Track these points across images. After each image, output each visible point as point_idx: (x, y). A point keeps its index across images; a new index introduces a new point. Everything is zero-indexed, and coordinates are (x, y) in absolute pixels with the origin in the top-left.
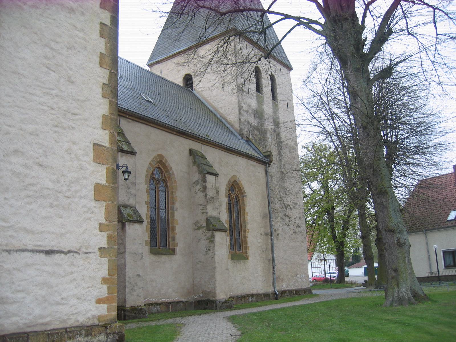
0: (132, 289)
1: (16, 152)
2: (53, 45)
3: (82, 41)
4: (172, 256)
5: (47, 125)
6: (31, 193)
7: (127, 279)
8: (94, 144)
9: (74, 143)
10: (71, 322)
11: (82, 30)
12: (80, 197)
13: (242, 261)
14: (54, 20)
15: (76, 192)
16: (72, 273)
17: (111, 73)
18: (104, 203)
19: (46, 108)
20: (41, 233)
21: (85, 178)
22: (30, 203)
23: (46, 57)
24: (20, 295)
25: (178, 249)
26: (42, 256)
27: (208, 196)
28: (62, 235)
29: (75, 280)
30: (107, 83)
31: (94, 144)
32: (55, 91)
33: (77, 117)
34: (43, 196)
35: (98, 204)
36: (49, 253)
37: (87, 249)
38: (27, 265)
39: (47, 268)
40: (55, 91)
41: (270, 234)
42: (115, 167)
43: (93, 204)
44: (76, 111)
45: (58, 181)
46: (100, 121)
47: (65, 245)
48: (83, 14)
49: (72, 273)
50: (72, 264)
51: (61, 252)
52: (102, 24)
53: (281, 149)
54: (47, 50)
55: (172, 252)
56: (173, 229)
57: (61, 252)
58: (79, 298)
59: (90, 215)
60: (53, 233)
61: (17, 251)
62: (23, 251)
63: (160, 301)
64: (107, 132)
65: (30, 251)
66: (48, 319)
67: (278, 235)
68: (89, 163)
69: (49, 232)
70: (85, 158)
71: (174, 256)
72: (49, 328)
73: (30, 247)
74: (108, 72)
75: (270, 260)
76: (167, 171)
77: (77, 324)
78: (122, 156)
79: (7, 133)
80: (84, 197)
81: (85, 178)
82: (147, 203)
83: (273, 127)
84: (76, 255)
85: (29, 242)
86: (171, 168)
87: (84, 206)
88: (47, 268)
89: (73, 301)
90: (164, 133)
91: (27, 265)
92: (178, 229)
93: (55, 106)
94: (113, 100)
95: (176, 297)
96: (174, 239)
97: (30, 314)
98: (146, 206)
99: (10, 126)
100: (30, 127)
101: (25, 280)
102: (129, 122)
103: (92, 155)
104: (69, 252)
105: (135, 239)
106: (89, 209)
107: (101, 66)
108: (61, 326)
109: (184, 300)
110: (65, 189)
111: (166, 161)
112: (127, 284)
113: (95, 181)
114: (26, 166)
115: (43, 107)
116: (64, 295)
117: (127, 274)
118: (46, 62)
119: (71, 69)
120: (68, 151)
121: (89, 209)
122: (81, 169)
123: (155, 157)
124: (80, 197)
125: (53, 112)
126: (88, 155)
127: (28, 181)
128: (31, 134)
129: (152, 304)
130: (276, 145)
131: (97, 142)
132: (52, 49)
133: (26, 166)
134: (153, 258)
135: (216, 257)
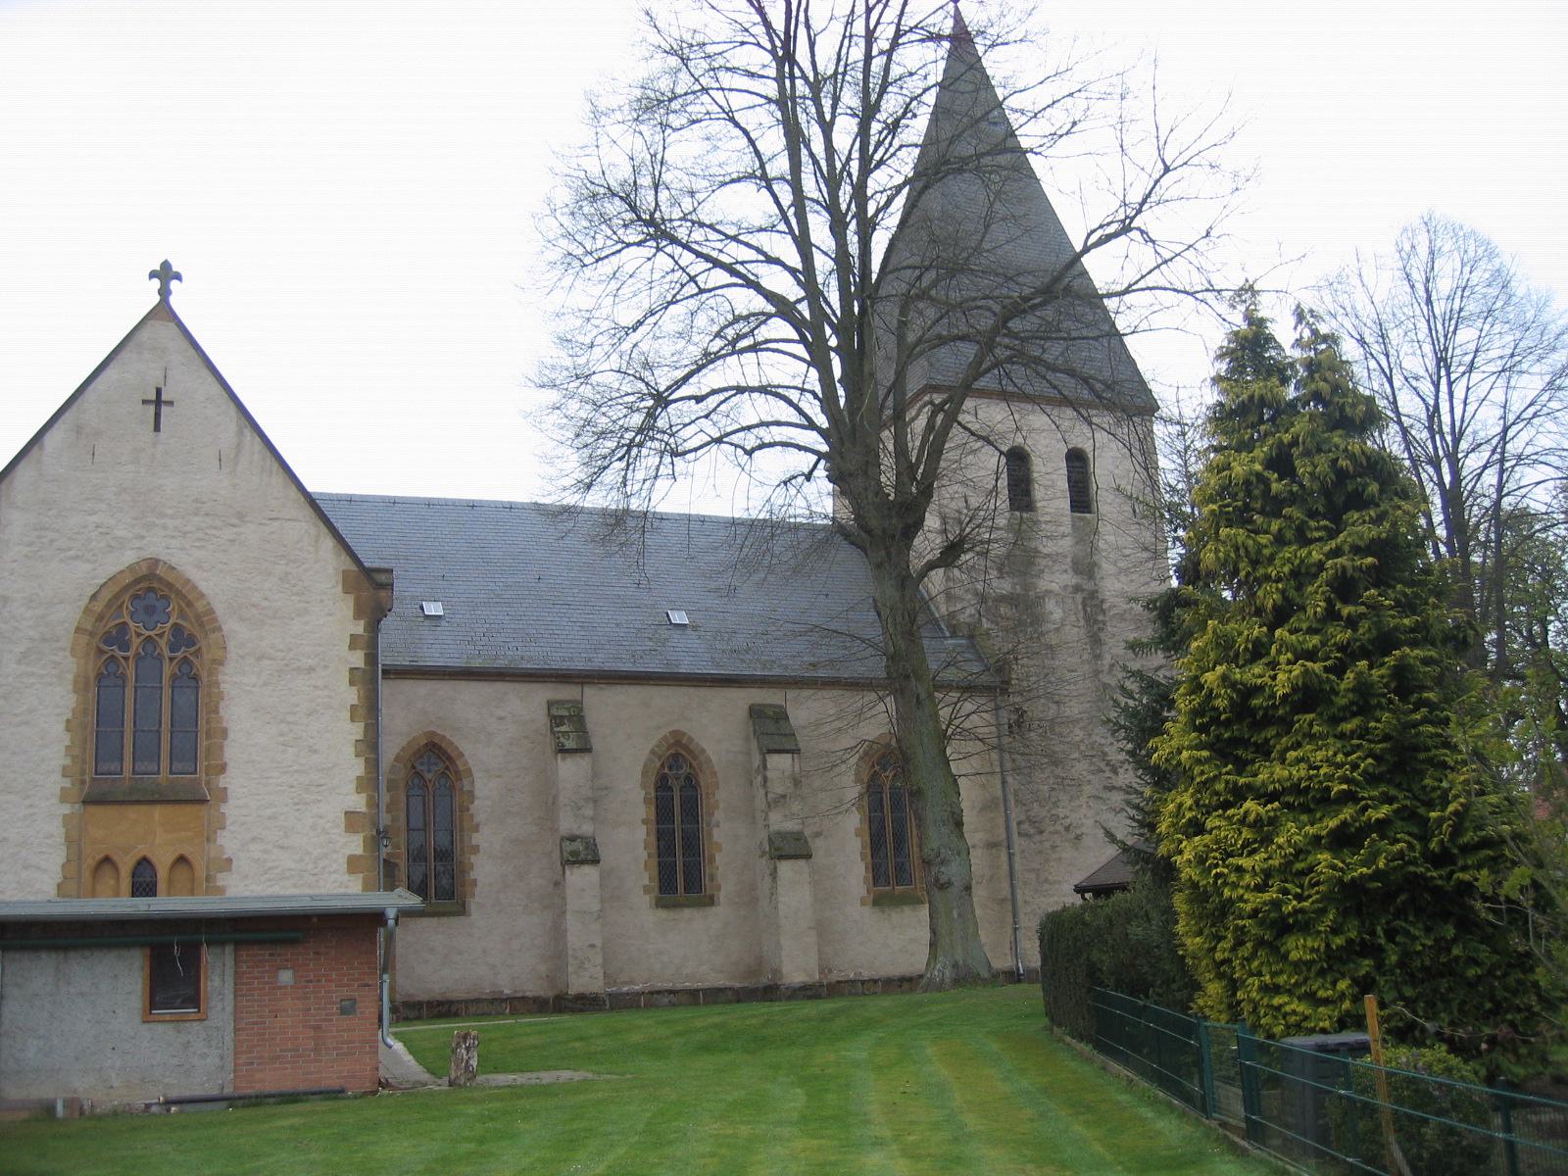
0: (580, 967)
1: (254, 839)
3: (326, 700)
4: (708, 908)
5: (286, 805)
7: (570, 952)
9: (321, 817)
11: (326, 687)
12: (330, 873)
13: (905, 908)
15: (324, 868)
18: (361, 875)
22: (271, 886)
25: (722, 896)
27: (769, 796)
30: (360, 737)
34: (287, 878)
35: (353, 877)
41: (1005, 844)
42: (374, 833)
43: (347, 877)
44: (322, 781)
46: (353, 786)
48: (326, 667)
53: (1101, 630)
55: (711, 901)
56: (712, 859)
63: (679, 986)
64: (364, 795)
67: (1078, 837)
68: (340, 835)
70: (335, 831)
71: (713, 909)
74: (362, 725)
75: (1003, 901)
76: (695, 758)
78: (564, 759)
80: (334, 872)
81: (335, 851)
82: (645, 822)
83: (1070, 579)
86: (703, 751)
87: (335, 882)
90: (684, 690)
92: (720, 859)
93: (295, 783)
94: (372, 756)
95: (719, 980)
96: (712, 878)
98: (645, 827)
100: (269, 812)
102: (602, 689)
105: (583, 890)
106: (341, 883)
109: (738, 985)
110: (310, 867)
111: (691, 740)
112: (570, 959)
113: (348, 852)
114: (265, 851)
117: (569, 945)
118: (281, 739)
119: (312, 738)
120: (313, 827)
123: (665, 738)
124: (330, 873)
129: (658, 992)
130: (1082, 623)
132: (289, 723)
133: (265, 851)
134: (662, 914)
135: (780, 906)
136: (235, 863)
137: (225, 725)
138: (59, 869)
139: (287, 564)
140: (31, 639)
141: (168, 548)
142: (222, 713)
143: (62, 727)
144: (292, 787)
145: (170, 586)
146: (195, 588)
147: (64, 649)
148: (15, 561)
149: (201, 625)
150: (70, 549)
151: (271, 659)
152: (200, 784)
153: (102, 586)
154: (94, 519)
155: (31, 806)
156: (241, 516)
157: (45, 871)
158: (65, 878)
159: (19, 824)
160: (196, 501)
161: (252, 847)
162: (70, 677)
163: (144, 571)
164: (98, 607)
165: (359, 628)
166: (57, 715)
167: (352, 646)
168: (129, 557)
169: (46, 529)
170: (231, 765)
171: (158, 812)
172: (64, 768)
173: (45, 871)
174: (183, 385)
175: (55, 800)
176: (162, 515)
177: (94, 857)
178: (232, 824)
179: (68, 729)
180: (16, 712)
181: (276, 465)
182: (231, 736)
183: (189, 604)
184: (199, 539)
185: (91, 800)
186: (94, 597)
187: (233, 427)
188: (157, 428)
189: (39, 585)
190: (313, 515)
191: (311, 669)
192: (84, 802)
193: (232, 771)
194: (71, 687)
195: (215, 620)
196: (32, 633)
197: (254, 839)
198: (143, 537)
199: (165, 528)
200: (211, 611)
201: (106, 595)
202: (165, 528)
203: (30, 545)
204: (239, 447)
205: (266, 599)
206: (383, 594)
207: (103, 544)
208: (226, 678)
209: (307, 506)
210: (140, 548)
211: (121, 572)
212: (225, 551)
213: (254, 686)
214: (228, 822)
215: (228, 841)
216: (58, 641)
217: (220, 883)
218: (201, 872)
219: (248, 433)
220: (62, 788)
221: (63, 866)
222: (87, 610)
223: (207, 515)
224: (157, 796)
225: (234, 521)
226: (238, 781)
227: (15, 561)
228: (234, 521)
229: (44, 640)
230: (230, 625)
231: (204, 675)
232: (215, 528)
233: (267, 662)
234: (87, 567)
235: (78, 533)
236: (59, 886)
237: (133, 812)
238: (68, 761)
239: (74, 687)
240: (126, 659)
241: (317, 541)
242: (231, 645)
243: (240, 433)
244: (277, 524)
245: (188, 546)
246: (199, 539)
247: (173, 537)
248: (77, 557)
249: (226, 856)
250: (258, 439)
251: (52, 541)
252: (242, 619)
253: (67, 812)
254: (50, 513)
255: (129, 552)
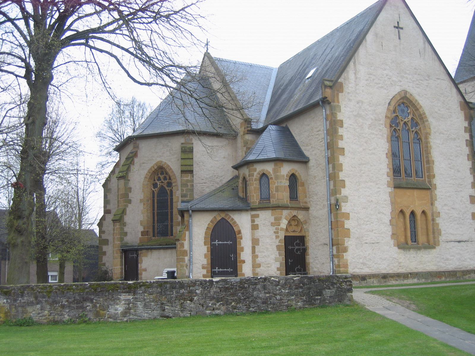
1: (445, 205)
2: (451, 158)
5: (453, 192)
6: (451, 220)
8: (470, 196)
9: (463, 197)
10: (468, 269)
12: (467, 219)
14: (449, 146)
16: (467, 249)
17: (472, 162)
19: (452, 185)
20: (456, 234)
21: (468, 211)
22: (451, 224)
23: (449, 164)
24: (452, 257)
26: (457, 243)
28: (462, 235)
29: (468, 252)
30: (471, 167)
31: (470, 196)
32: (454, 177)
33: (462, 186)
34: (455, 221)
36: (459, 242)
37: (471, 239)
38: (453, 247)
39: (459, 248)
40: (454, 177)
45: (459, 214)
46: (470, 186)
47: (464, 238)
48: (459, 139)
49: (467, 249)
50: (467, 246)
51: (463, 241)
52: (467, 140)
54: (449, 161)
57: (463, 241)
58: (470, 259)
59: (471, 226)
60: (460, 234)
61: (450, 242)
62: (452, 241)
65: (453, 241)
66: (461, 266)
68: (468, 204)
69: (458, 234)
72: (462, 270)
73: (453, 240)
74: (471, 162)
77: (470, 269)
79: (442, 198)
84: (468, 242)
85: (453, 238)
87: (469, 223)
88: (459, 248)
89: (469, 260)
91: (453, 247)
93: (455, 183)
97: (455, 264)
99: (442, 195)
100: (448, 194)
101: (453, 252)
103: (469, 201)
104: (466, 241)
106: (470, 223)
107: (468, 160)
108: (465, 269)
110: (461, 216)
114: (449, 210)
115: (451, 185)
116: (465, 258)
118: (449, 166)
119: (458, 166)
120: (461, 201)
121: (470, 223)
122: (466, 207)
124: (467, 219)
125: (455, 186)
126: (468, 201)
127: (450, 215)
128: (449, 197)
131: (470, 195)
132: (451, 160)
136: (441, 214)
137: (433, 159)
138: (390, 214)
139: (444, 97)
140: (372, 119)
141: (409, 87)
142: (432, 154)
143: (385, 156)
144: (454, 185)
145: (411, 102)
146: (419, 103)
147: (382, 124)
148: (363, 86)
149: (422, 119)
150: (379, 84)
151: (443, 134)
152: (426, 182)
153: (392, 99)
154: (385, 72)
155: (379, 188)
156: (429, 76)
157: (385, 215)
158: (392, 218)
159: (375, 195)
160: (415, 69)
161: (445, 208)
162: (386, 136)
163: (403, 95)
164: (392, 108)
165: (466, 124)
166: (383, 151)
167: (465, 131)
168: (398, 89)
169: (371, 75)
170: (436, 175)
171: (416, 193)
172: (388, 173)
173: (385, 215)
174: (406, 22)
175: (386, 186)
176: (406, 73)
177: (398, 210)
178: (439, 198)
179: (387, 157)
180: (371, 148)
181: (436, 58)
182: (435, 163)
183: (417, 110)
184: (417, 84)
185: (397, 187)
186: (389, 104)
187: (422, 41)
188: (399, 38)
189: (372, 97)
190: (449, 79)
191: (455, 139)
192: (394, 187)
193: (437, 177)
194: (386, 140)
195: (426, 117)
196: (372, 117)
197: (445, 205)
198: (401, 81)
199: (407, 78)
200: (424, 114)
201: (393, 104)
202: (407, 78)
203: (367, 80)
204: (424, 48)
205: (439, 110)
206: (472, 111)
207: (389, 83)
208: (432, 140)
209: (447, 75)
210: (401, 86)
211: (396, 95)
212: (425, 90)
213: (440, 144)
214: (437, 198)
215: (439, 205)
216: (380, 121)
217: (437, 222)
218: (430, 218)
219: (427, 44)
220: (387, 181)
221: (391, 213)
222: (388, 109)
223: (419, 75)
224: (415, 186)
225: (427, 78)
226: (437, 181)
227: (363, 86)
228: (427, 78)
229: (376, 120)
230: (430, 119)
231: (423, 138)
232: (422, 80)
233: (443, 135)
234: (386, 91)
235: (381, 77)
236: (390, 221)
237: (409, 192)
238: (388, 170)
239: (387, 140)
240: (399, 130)
241: (451, 89)
242: (432, 127)
243: (424, 43)
244: (439, 81)
245: (414, 86)
246: (417, 84)
247: (410, 82)
248: (382, 87)
249: (438, 211)
250: (430, 47)
251: (373, 80)
252: (434, 118)
253: (390, 191)
254: (372, 68)
255: (397, 87)
